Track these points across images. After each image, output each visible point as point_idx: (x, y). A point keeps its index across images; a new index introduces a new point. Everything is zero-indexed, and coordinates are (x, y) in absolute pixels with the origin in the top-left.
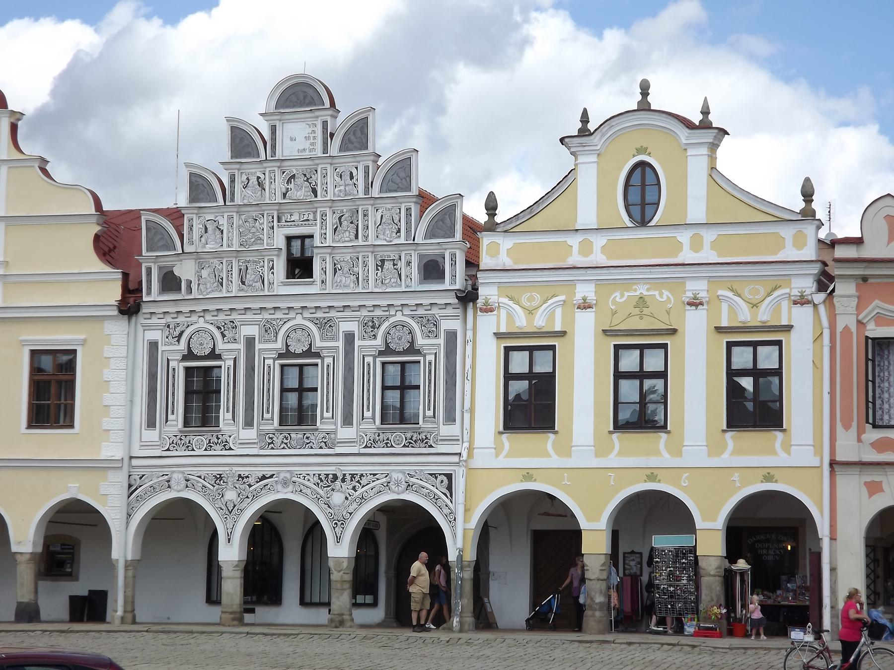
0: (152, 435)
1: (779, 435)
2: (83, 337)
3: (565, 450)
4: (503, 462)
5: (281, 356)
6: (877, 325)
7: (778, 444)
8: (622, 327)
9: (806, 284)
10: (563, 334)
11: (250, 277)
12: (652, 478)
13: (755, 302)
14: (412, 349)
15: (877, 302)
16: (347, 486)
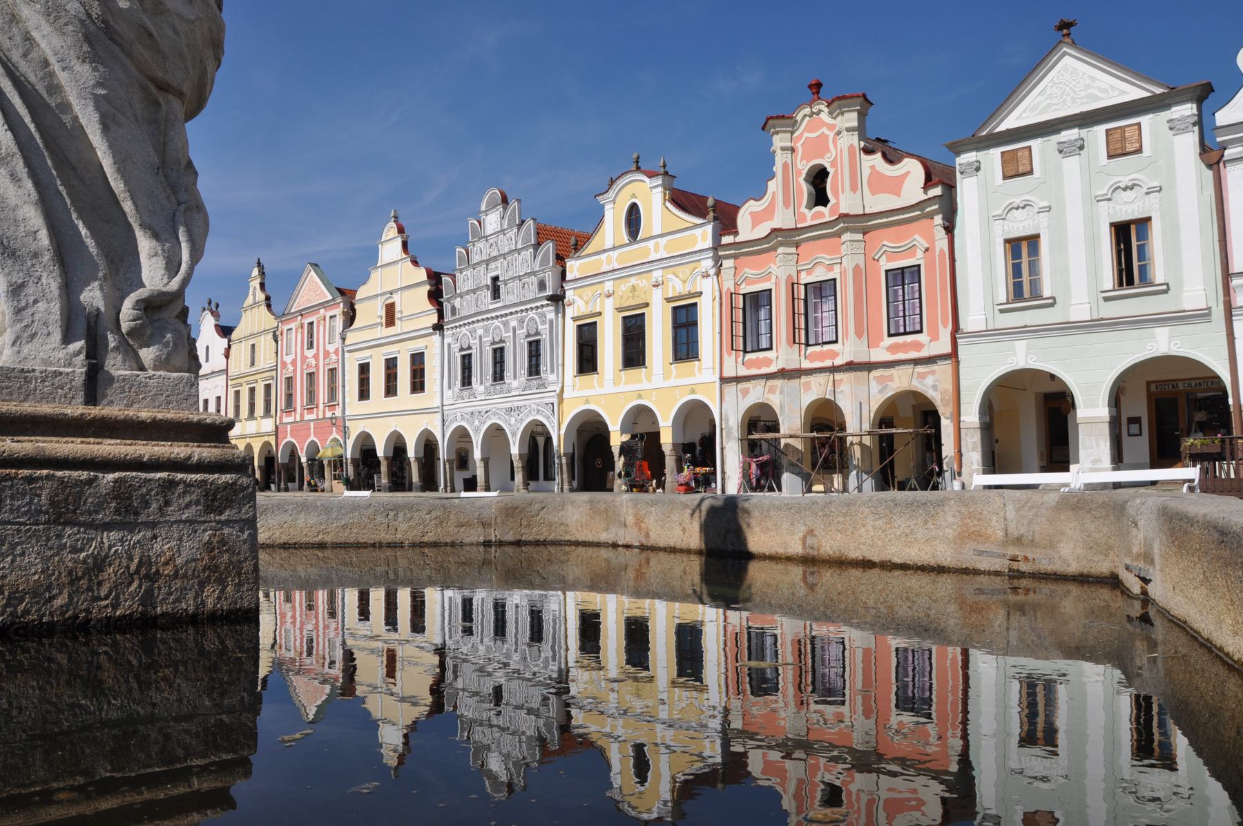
0: (448, 393)
1: (697, 363)
2: (424, 345)
3: (601, 385)
4: (577, 394)
5: (492, 344)
6: (746, 285)
7: (696, 369)
8: (625, 305)
9: (707, 264)
10: (600, 314)
11: (479, 302)
12: (640, 396)
13: (684, 279)
14: (537, 333)
15: (747, 270)
16: (516, 414)
